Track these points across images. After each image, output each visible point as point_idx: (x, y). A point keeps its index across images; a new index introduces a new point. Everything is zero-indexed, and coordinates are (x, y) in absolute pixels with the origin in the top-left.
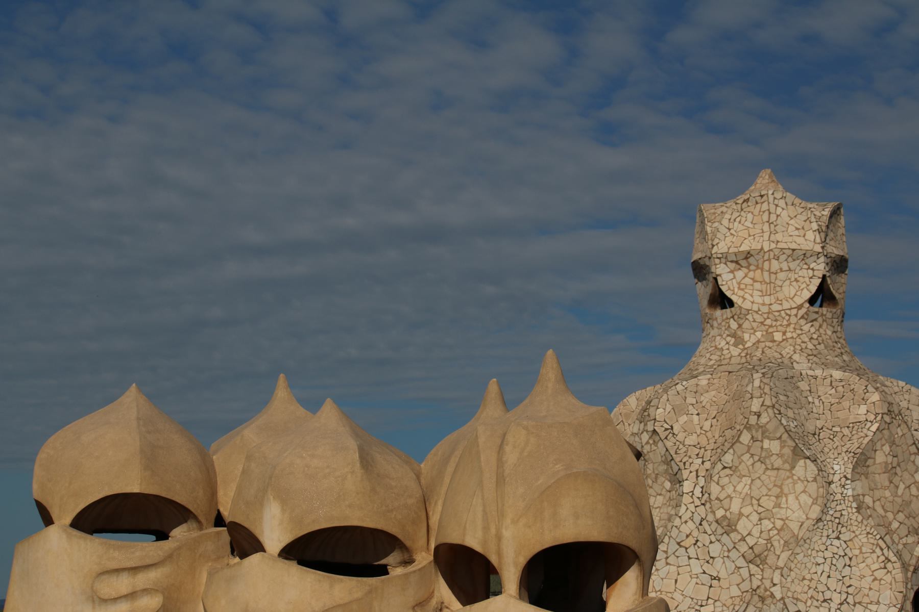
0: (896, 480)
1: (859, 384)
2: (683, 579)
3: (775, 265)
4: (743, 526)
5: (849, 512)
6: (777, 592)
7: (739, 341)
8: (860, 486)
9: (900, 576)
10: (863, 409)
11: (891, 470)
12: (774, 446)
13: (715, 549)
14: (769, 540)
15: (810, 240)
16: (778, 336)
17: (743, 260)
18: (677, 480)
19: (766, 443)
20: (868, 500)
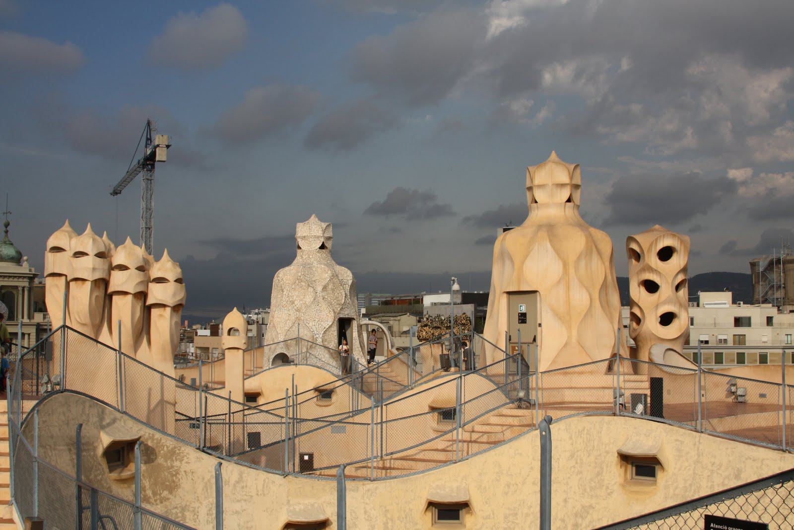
0: (335, 292)
1: (327, 269)
2: (283, 315)
3: (311, 240)
4: (296, 303)
5: (321, 299)
6: (302, 318)
7: (302, 257)
8: (324, 294)
9: (333, 314)
10: (327, 275)
11: (333, 290)
12: (303, 284)
13: (290, 308)
14: (302, 306)
15: (320, 233)
16: (311, 257)
17: (304, 238)
18: (283, 291)
19: (302, 283)
20: (326, 297)
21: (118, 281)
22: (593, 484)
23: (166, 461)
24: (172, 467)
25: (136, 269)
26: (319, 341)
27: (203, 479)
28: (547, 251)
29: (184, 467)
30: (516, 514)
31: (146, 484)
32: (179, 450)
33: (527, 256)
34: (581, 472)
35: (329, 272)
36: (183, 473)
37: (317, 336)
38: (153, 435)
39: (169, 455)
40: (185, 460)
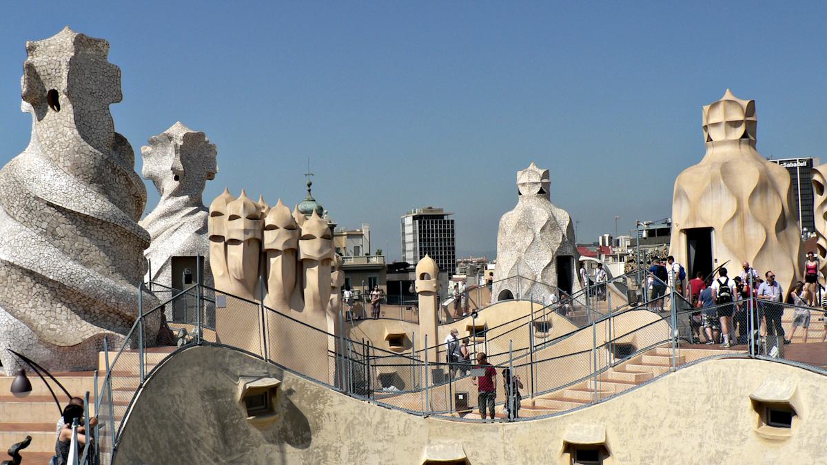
5: (539, 240)
12: (523, 226)
15: (538, 180)
17: (523, 184)
21: (271, 240)
22: (727, 430)
23: (310, 405)
24: (315, 409)
25: (285, 228)
26: (539, 278)
27: (346, 420)
28: (721, 188)
29: (328, 410)
30: (652, 457)
31: (288, 427)
32: (323, 394)
33: (687, 196)
34: (716, 417)
35: (547, 215)
36: (326, 415)
37: (537, 273)
38: (297, 380)
39: (312, 398)
40: (329, 402)
